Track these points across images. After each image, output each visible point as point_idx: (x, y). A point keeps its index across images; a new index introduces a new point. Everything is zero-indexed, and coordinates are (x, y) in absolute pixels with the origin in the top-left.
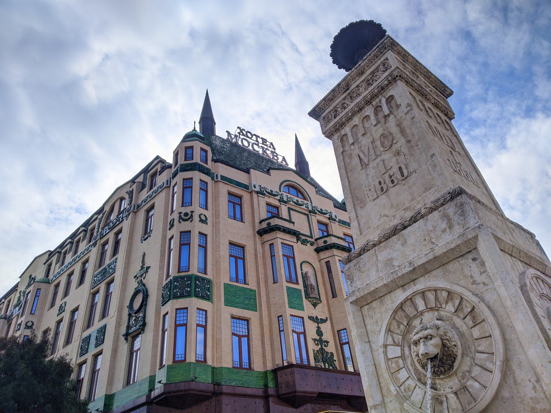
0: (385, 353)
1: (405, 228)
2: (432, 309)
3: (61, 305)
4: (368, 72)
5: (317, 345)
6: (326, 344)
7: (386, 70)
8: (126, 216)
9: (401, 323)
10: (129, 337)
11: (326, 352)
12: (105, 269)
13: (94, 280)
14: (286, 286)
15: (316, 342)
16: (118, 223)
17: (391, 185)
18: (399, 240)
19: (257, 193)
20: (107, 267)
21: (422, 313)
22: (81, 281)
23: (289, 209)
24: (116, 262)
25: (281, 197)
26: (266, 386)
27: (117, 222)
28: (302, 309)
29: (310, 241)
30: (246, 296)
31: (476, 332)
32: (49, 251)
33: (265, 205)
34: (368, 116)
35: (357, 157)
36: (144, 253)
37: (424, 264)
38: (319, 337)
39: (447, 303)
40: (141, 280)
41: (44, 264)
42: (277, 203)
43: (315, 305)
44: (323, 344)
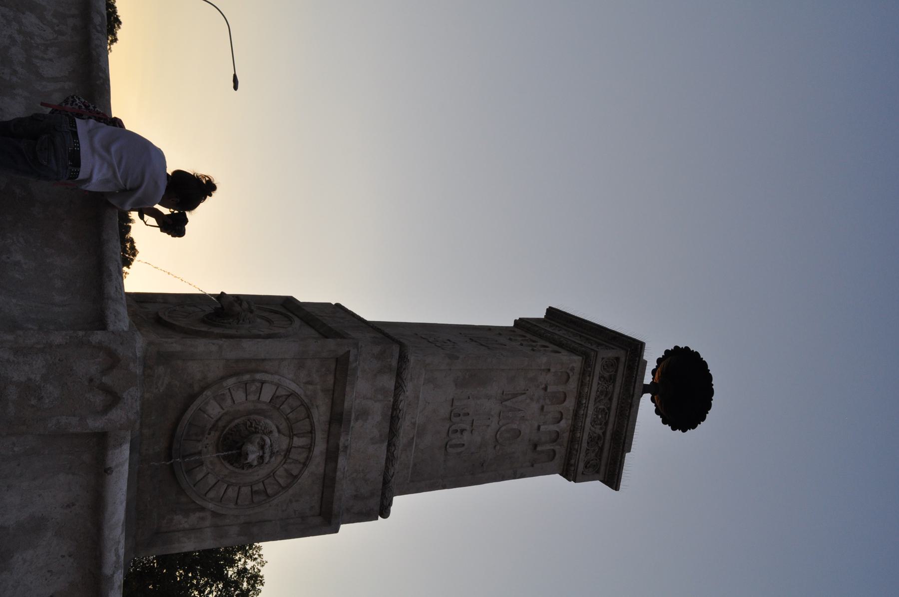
0: (272, 383)
1: (389, 445)
2: (288, 451)
4: (607, 446)
7: (586, 467)
9: (292, 411)
17: (454, 427)
18: (381, 436)
21: (291, 438)
31: (246, 490)
34: (559, 422)
35: (524, 390)
37: (336, 462)
39: (286, 470)
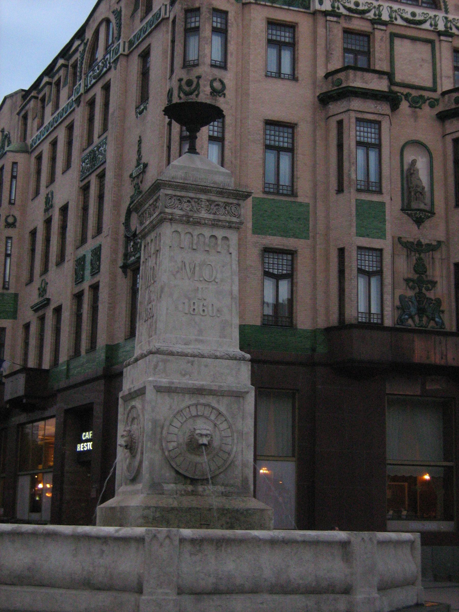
3: (48, 195)
5: (412, 288)
6: (429, 286)
8: (115, 61)
10: (128, 270)
11: (427, 298)
12: (93, 151)
13: (83, 168)
14: (356, 200)
15: (411, 284)
16: (105, 69)
19: (326, 13)
20: (96, 149)
22: (68, 165)
23: (393, 36)
24: (106, 143)
25: (377, 13)
26: (313, 350)
27: (103, 67)
28: (383, 236)
29: (429, 99)
30: (290, 216)
32: (23, 90)
33: (340, 34)
36: (140, 137)
38: (418, 275)
40: (138, 184)
41: (18, 114)
42: (364, 26)
43: (419, 222)
44: (425, 286)
